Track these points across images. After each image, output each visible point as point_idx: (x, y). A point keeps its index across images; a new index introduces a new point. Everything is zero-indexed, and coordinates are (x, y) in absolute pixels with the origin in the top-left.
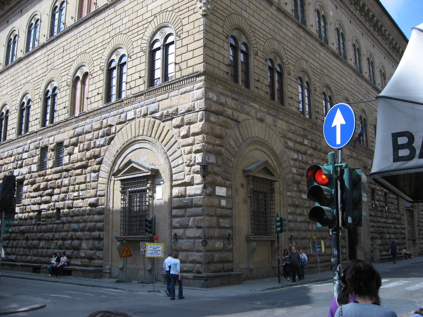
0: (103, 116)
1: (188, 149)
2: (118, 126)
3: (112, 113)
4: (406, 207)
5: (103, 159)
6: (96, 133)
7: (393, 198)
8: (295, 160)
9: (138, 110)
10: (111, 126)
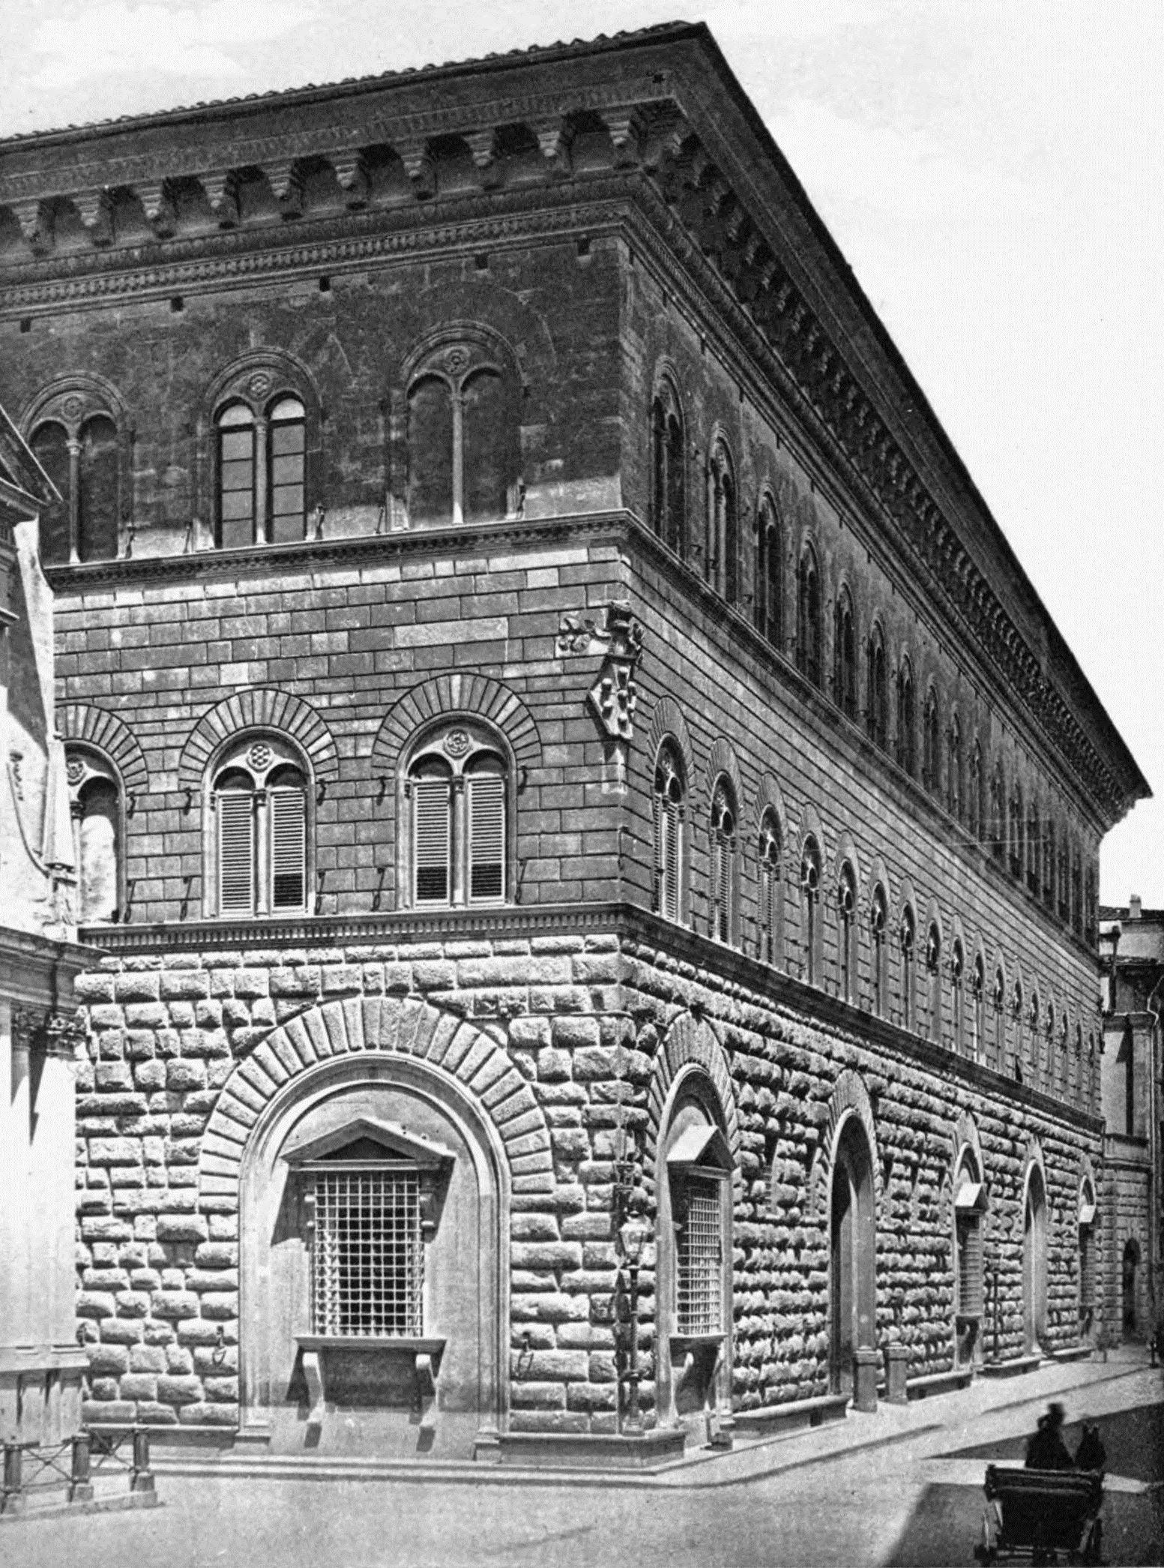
0: (212, 957)
1: (574, 1113)
2: (282, 1003)
3: (255, 956)
4: (957, 1208)
5: (217, 1096)
6: (183, 1009)
7: (931, 1183)
8: (749, 1108)
9: (370, 967)
10: (249, 998)
